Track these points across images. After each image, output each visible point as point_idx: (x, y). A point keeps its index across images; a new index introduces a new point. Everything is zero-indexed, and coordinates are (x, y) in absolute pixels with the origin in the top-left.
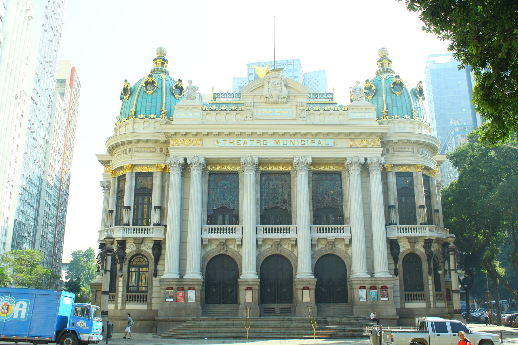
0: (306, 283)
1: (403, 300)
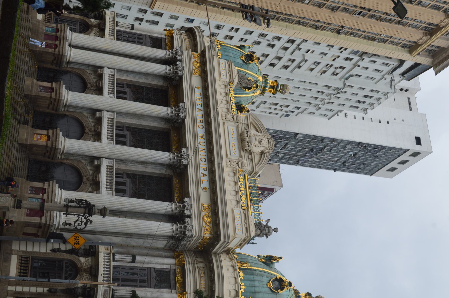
0: (54, 138)
1: (21, 254)
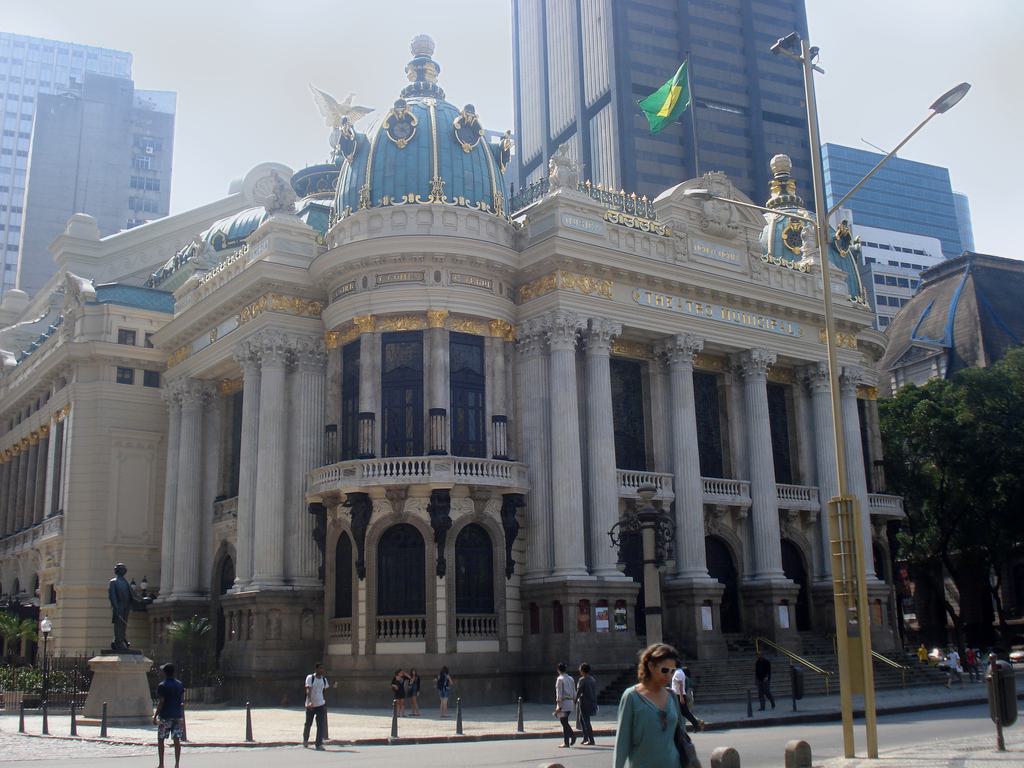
0: (786, 592)
